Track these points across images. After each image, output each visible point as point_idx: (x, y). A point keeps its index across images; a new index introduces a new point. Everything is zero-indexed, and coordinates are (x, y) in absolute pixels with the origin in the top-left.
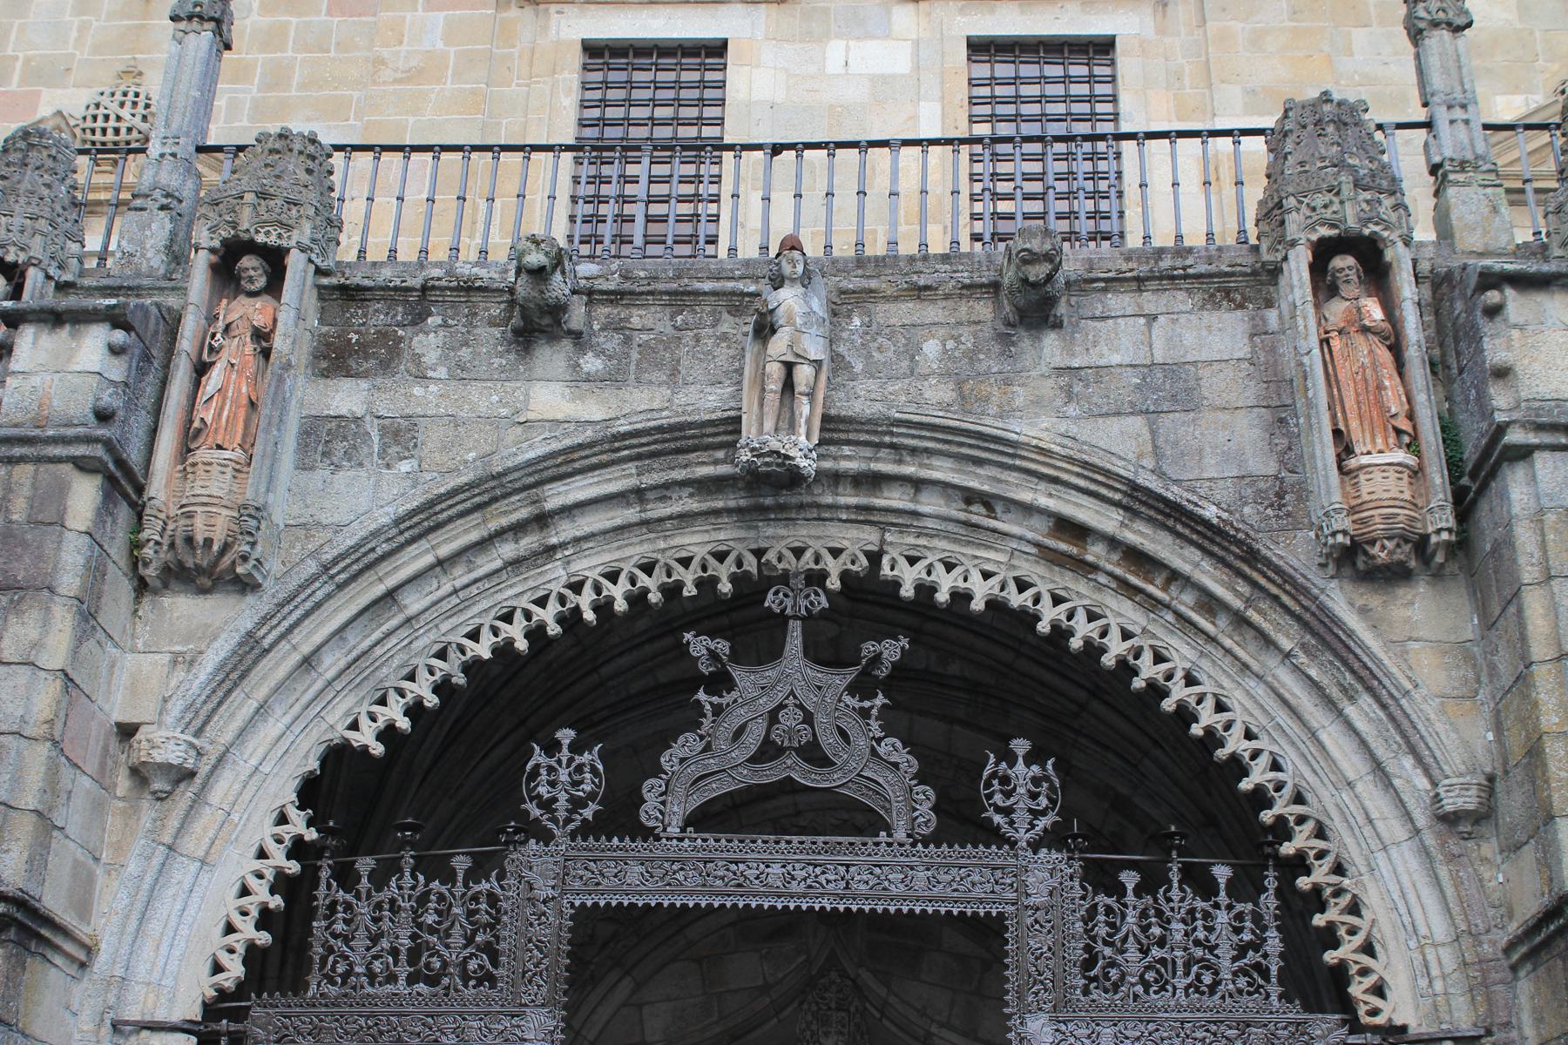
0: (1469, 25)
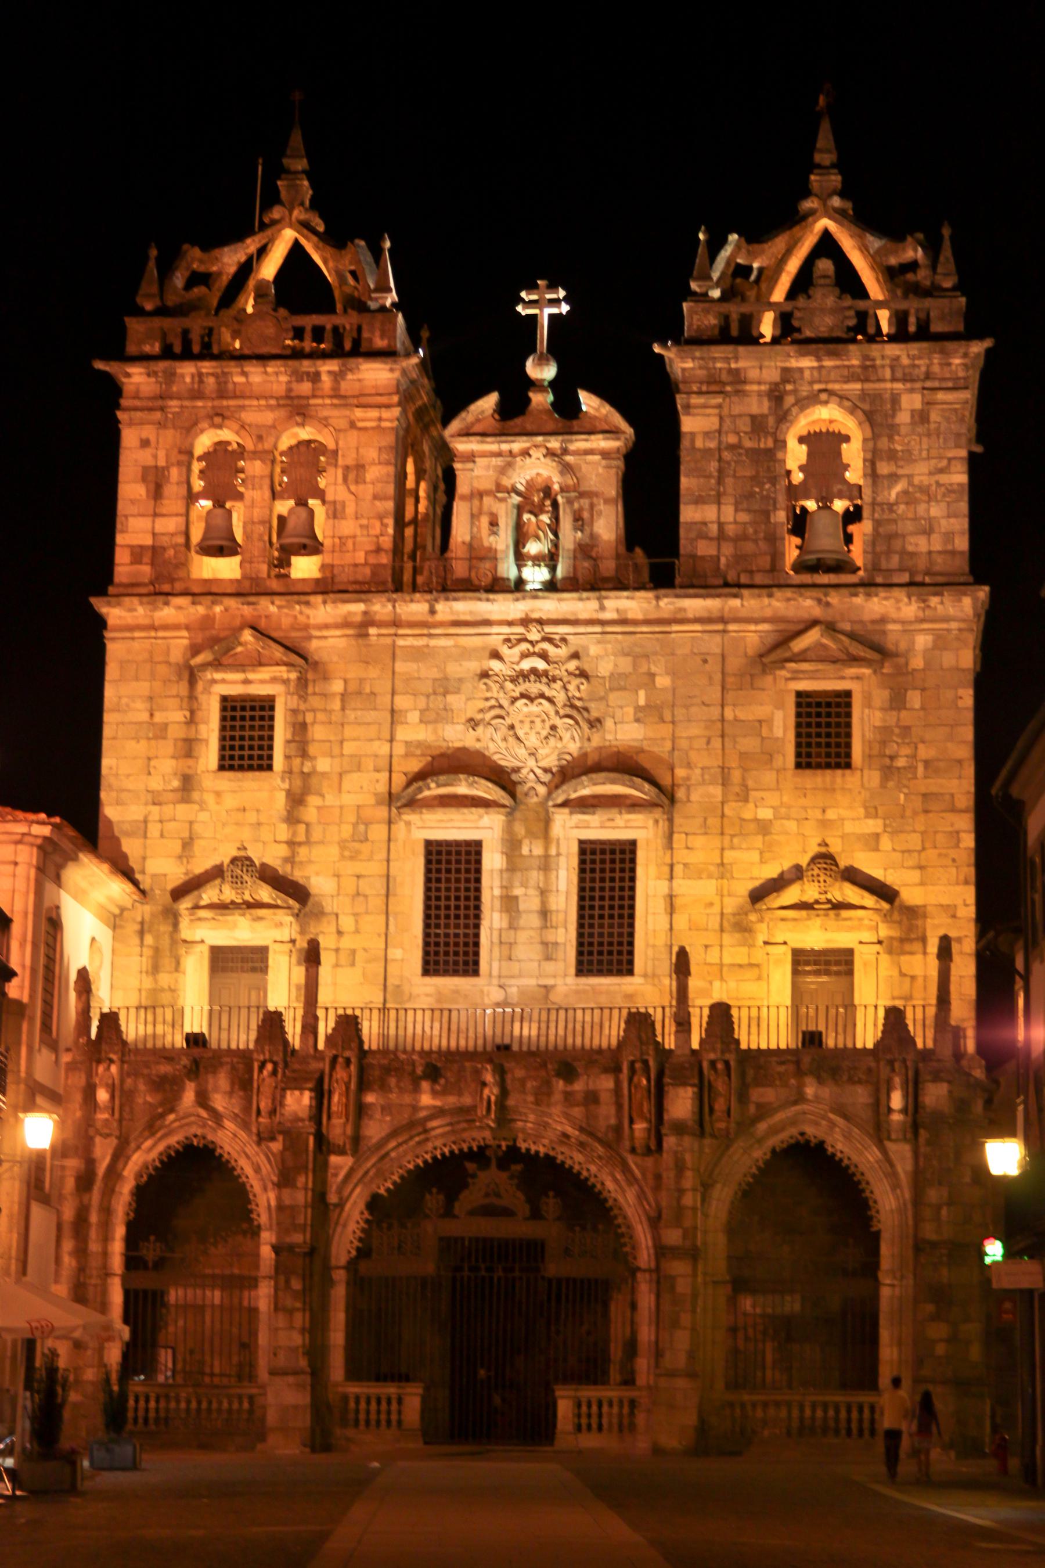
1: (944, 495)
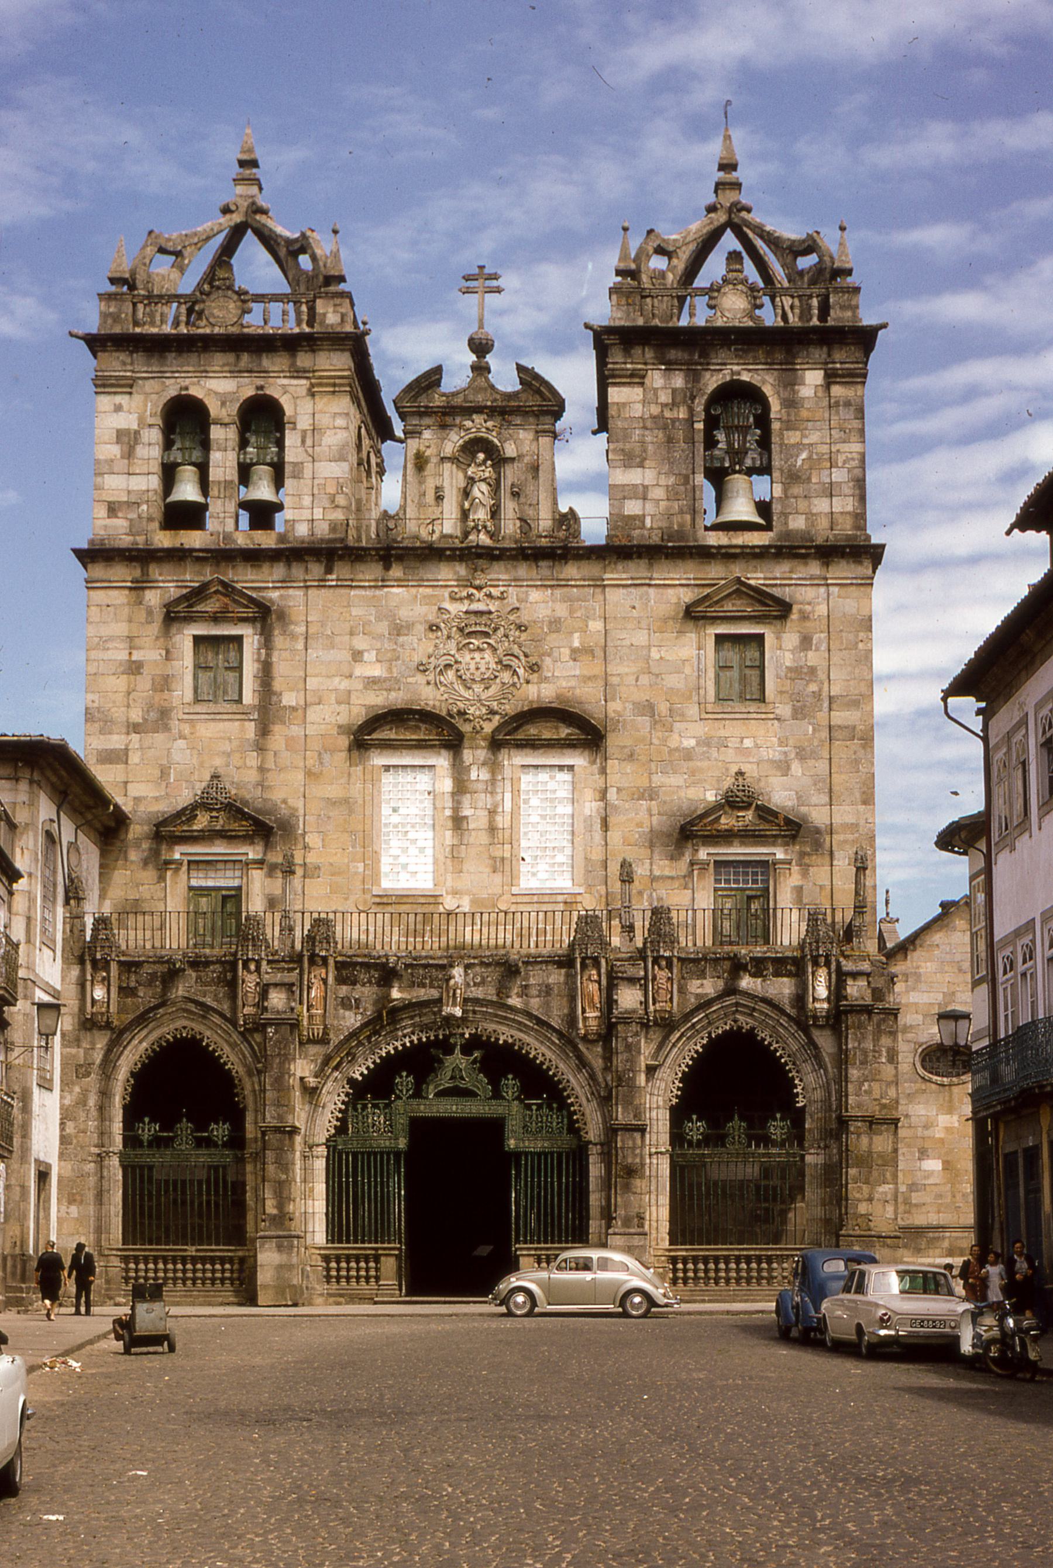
1: (844, 462)
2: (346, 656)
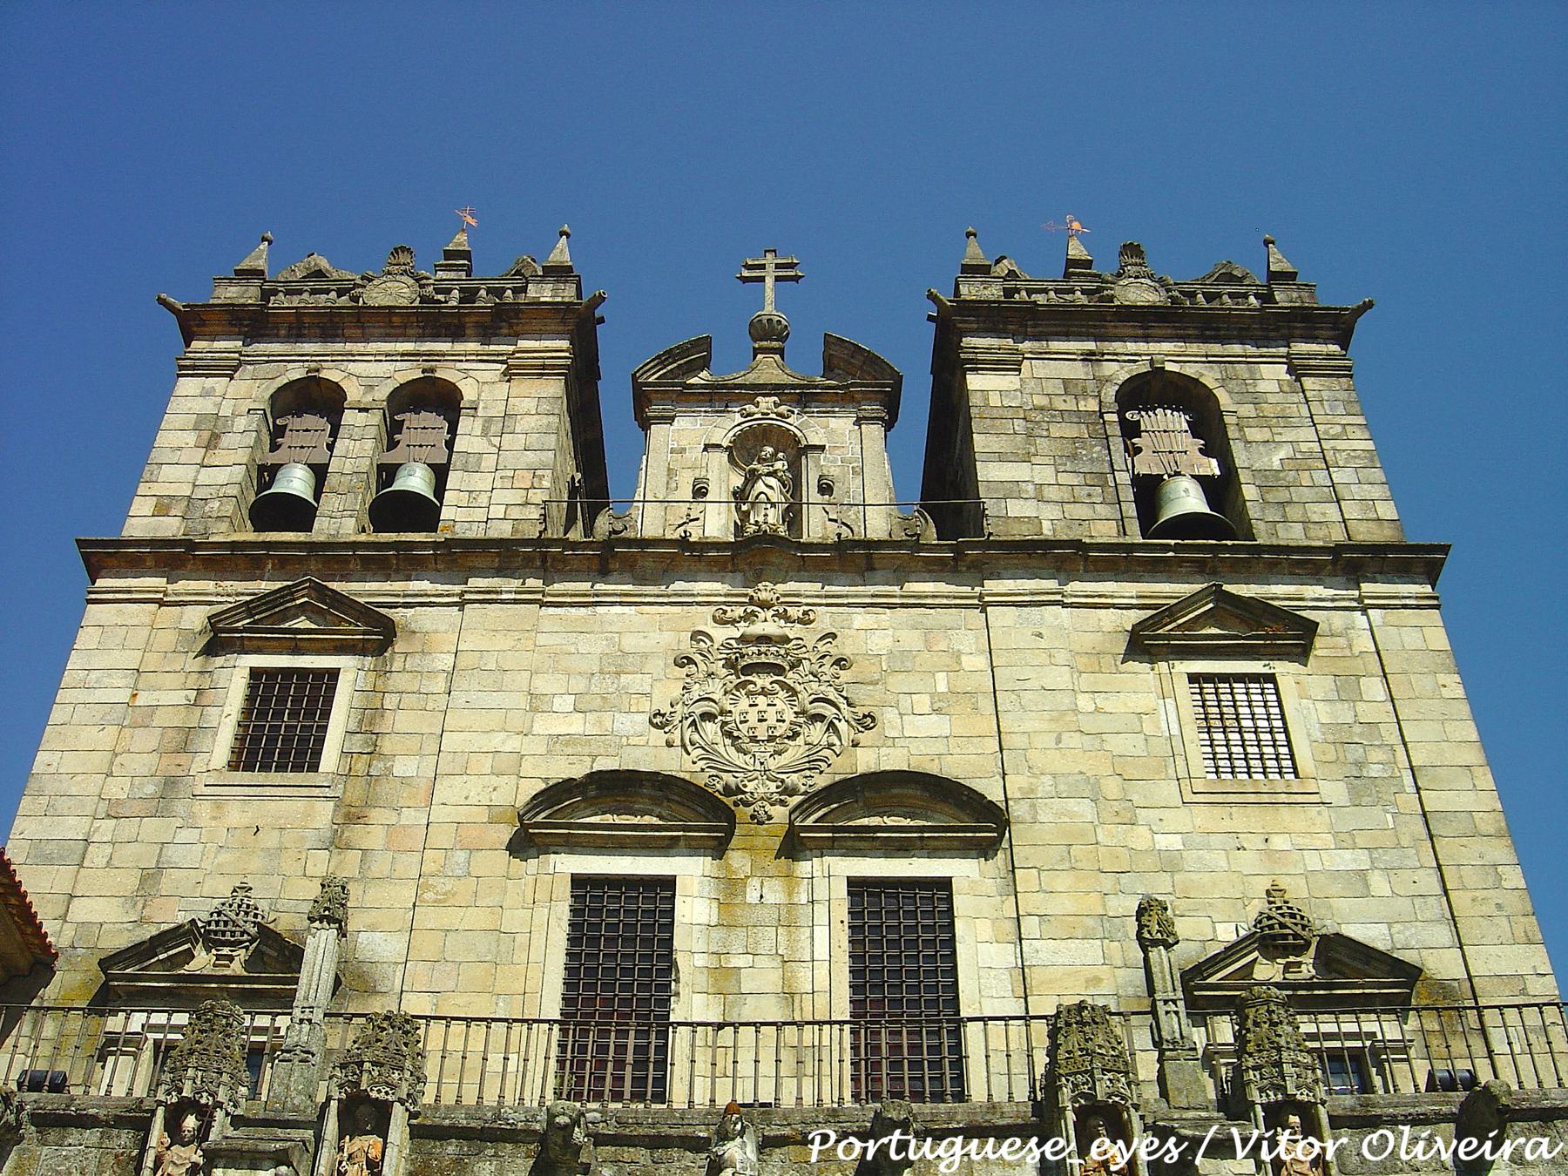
0: (1177, 942)
2: (522, 701)
